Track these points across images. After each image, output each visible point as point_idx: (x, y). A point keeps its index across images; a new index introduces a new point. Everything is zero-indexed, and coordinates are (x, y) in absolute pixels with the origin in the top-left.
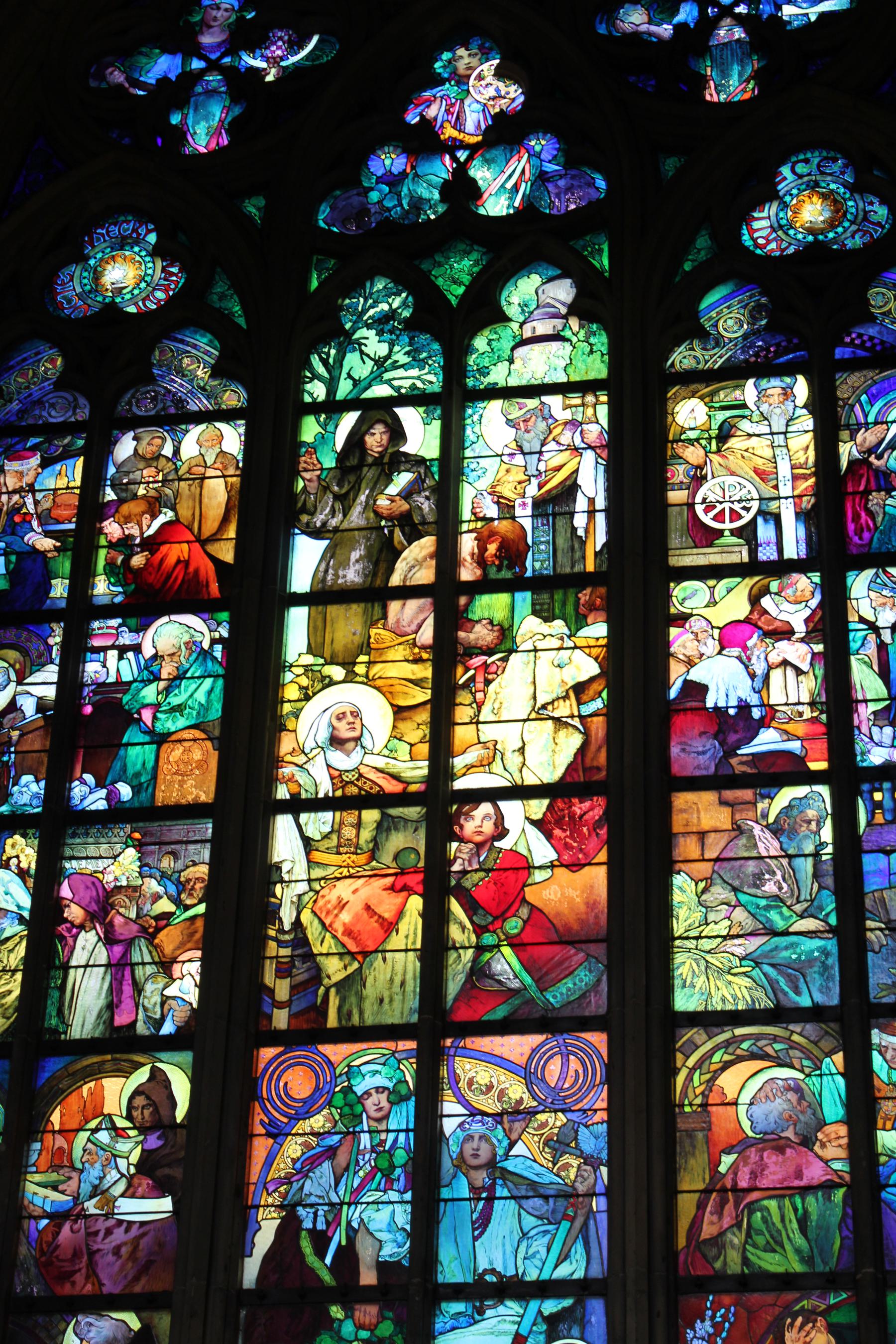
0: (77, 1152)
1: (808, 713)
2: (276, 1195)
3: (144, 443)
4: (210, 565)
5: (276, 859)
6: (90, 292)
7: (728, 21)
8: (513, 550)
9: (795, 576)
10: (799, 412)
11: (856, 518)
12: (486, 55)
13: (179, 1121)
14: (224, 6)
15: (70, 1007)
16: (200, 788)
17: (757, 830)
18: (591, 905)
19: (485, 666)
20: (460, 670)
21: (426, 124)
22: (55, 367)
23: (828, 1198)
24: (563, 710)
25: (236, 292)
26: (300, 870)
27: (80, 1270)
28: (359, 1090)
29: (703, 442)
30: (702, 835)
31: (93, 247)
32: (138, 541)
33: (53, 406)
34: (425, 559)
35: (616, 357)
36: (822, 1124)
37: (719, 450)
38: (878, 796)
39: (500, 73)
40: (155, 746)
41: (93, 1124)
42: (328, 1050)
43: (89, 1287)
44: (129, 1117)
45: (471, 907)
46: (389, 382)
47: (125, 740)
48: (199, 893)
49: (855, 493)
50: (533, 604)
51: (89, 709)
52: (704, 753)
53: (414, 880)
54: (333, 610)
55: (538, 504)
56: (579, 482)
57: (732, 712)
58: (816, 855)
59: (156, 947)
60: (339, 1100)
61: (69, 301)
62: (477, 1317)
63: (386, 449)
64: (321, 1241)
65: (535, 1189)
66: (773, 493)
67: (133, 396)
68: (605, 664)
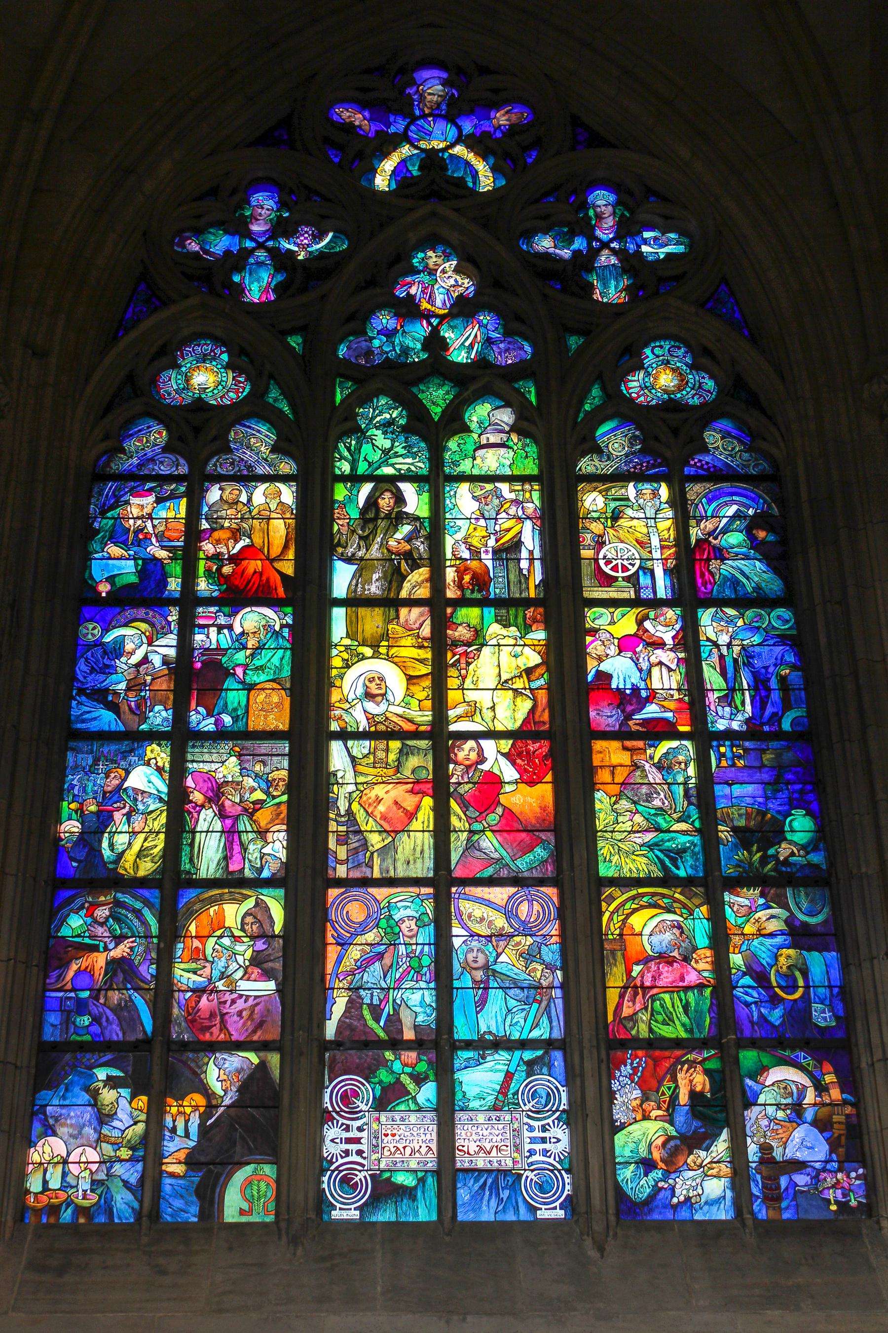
0: (209, 951)
3: (227, 492)
4: (278, 577)
5: (332, 769)
7: (606, 251)
9: (665, 609)
11: (702, 575)
12: (447, 257)
16: (280, 721)
17: (647, 766)
18: (544, 809)
19: (466, 653)
20: (449, 655)
23: (701, 993)
24: (519, 684)
25: (285, 397)
26: (350, 777)
28: (397, 917)
30: (614, 767)
33: (162, 463)
34: (423, 582)
36: (695, 949)
37: (612, 527)
38: (722, 749)
39: (457, 270)
41: (218, 933)
42: (373, 891)
43: (222, 1036)
44: (243, 929)
45: (464, 806)
46: (392, 465)
48: (282, 786)
49: (701, 560)
51: (199, 665)
54: (362, 611)
55: (495, 552)
57: (628, 692)
58: (685, 784)
59: (255, 821)
60: (383, 923)
61: (169, 394)
65: (516, 984)
66: (648, 556)
68: (545, 656)
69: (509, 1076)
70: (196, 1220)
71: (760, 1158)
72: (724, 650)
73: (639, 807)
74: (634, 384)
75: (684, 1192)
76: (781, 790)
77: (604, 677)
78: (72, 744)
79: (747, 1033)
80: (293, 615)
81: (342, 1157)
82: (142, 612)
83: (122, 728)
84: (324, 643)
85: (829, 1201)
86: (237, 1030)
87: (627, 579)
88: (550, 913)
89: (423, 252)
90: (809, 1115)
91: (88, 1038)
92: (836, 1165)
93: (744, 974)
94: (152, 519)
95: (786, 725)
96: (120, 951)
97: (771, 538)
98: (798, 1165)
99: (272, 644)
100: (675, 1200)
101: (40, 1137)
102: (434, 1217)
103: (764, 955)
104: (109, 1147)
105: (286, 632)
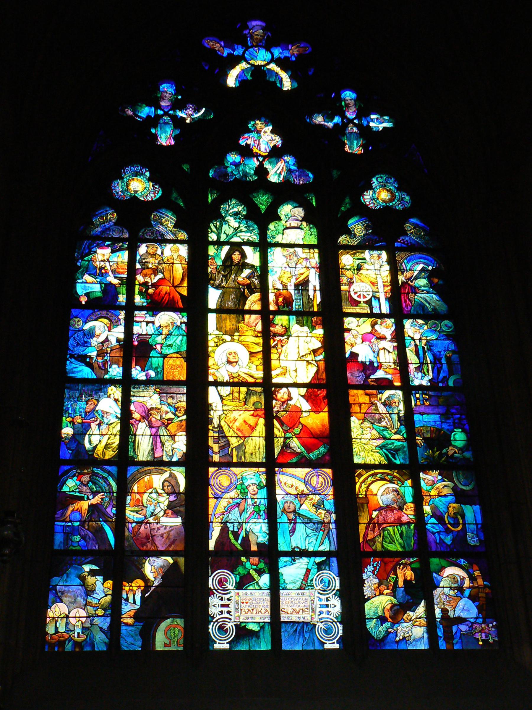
0: (144, 501)
1: (393, 366)
2: (219, 518)
3: (150, 248)
4: (178, 295)
6: (125, 191)
7: (351, 125)
8: (288, 301)
9: (386, 319)
10: (384, 263)
11: (405, 301)
12: (267, 125)
13: (181, 491)
14: (168, 92)
15: (138, 449)
18: (323, 426)
19: (281, 341)
20: (272, 341)
21: (248, 145)
22: (114, 217)
27: (149, 542)
28: (246, 484)
29: (352, 270)
30: (360, 405)
31: (125, 174)
32: (150, 284)
33: (114, 231)
35: (320, 236)
36: (405, 503)
37: (357, 274)
38: (418, 396)
39: (272, 132)
40: (162, 358)
41: (150, 491)
42: (233, 469)
45: (282, 424)
46: (239, 236)
47: (151, 355)
48: (183, 412)
49: (404, 293)
50: (296, 321)
52: (359, 376)
53: (261, 413)
54: (224, 316)
56: (310, 279)
57: (368, 363)
59: (168, 430)
60: (239, 487)
61: (118, 193)
62: (293, 562)
63: (240, 260)
64: (236, 535)
65: (310, 521)
66: (377, 290)
67: (145, 231)
69: (308, 571)
70: (140, 649)
71: (442, 616)
72: (417, 342)
73: (374, 426)
74: (367, 198)
75: (402, 634)
76: (449, 419)
77: (354, 355)
78: (68, 385)
79: (434, 549)
80: (187, 317)
81: (219, 615)
82: (104, 313)
83: (95, 377)
84: (204, 334)
85: (478, 640)
86: (161, 545)
87: (366, 302)
88: (328, 483)
89: (253, 120)
90: (467, 593)
91: (79, 548)
92: (481, 620)
93: (431, 517)
94: (109, 262)
95: (451, 383)
96: (96, 500)
97: (441, 282)
98: (461, 620)
99: (176, 332)
100: (398, 639)
101: (53, 603)
102: (269, 648)
103: (441, 507)
104: (92, 608)
105: (183, 326)
